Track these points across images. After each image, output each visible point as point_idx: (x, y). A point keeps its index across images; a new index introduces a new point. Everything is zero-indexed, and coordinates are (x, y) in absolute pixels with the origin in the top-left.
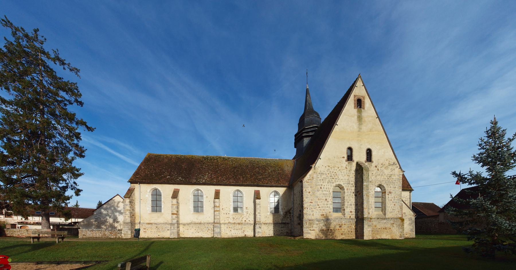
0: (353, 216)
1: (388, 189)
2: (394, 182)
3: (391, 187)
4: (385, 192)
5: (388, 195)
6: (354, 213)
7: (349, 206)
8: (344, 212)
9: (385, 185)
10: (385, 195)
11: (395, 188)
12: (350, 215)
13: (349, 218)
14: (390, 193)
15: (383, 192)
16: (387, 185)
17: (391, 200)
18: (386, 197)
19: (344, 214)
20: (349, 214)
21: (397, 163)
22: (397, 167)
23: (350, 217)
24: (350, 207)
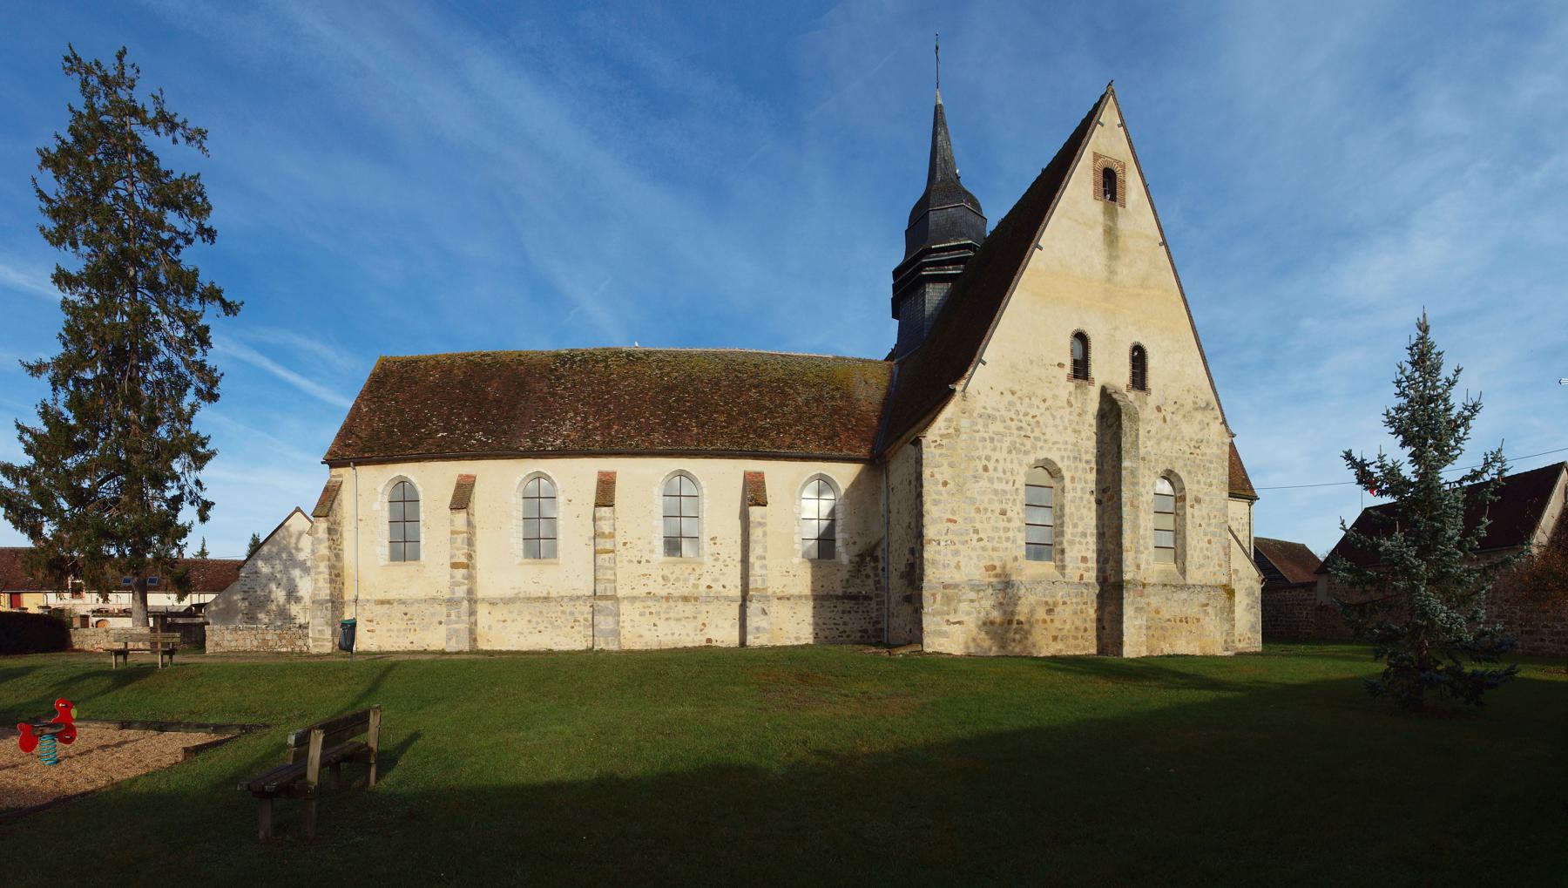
0: (1091, 576)
1: (1191, 488)
2: (1208, 465)
3: (1199, 482)
4: (1183, 499)
5: (1192, 507)
6: (1093, 564)
7: (1077, 539)
8: (1062, 561)
9: (1183, 475)
10: (1184, 507)
11: (1211, 485)
12: (1081, 572)
13: (1076, 580)
14: (1198, 500)
15: (1178, 495)
16: (1189, 472)
17: (1200, 526)
18: (1185, 513)
19: (1063, 567)
20: (1079, 569)
21: (1217, 407)
22: (1217, 418)
23: (1081, 577)
24: (1080, 543)
